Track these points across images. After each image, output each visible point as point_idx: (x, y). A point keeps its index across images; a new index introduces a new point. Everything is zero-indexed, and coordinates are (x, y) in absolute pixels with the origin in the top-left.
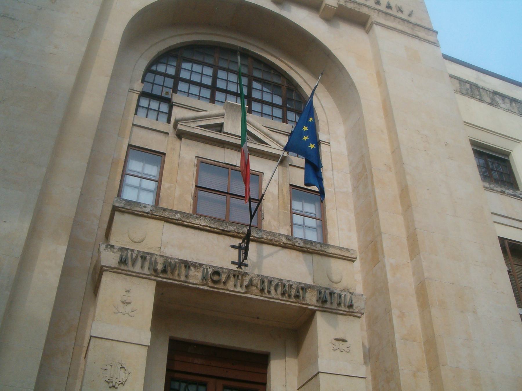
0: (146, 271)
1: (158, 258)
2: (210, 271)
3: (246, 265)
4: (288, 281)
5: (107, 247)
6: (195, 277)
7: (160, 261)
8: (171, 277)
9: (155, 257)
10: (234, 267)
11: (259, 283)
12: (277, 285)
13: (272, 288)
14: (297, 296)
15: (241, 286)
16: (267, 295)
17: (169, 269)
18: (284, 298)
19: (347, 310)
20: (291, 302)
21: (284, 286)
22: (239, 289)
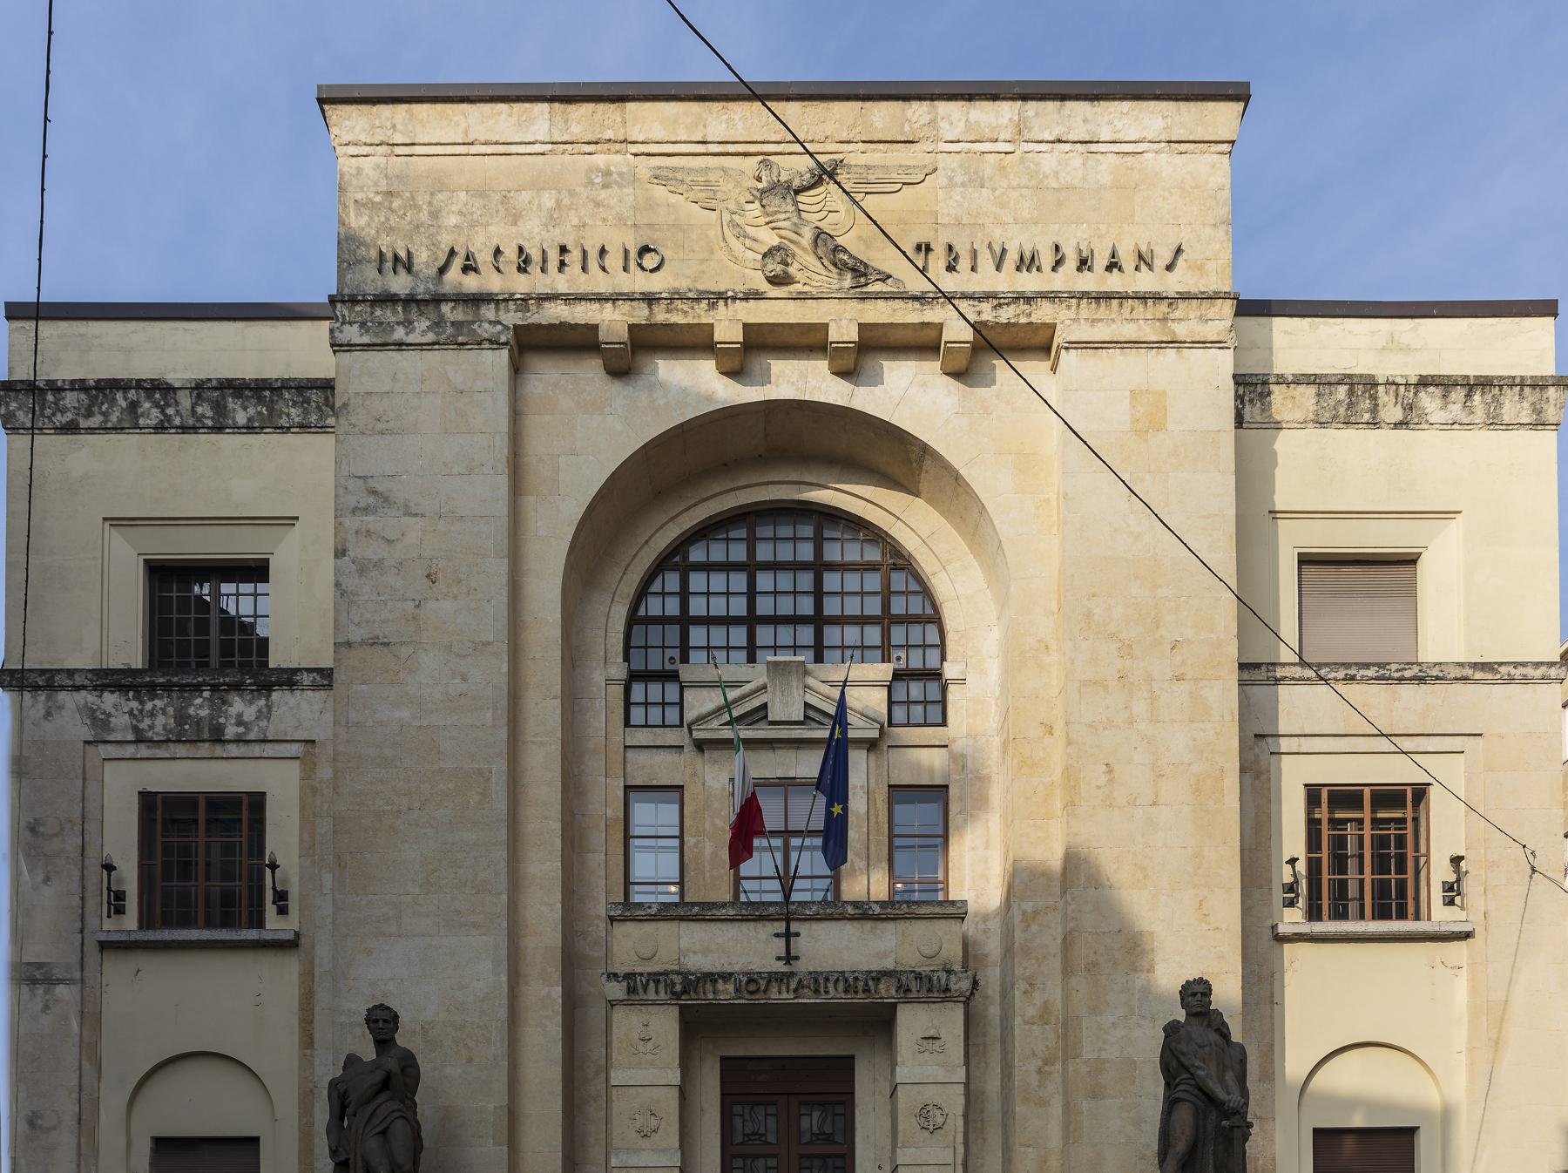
2: (744, 979)
3: (797, 958)
6: (726, 992)
7: (678, 979)
13: (831, 986)
14: (866, 990)
20: (861, 999)
22: (785, 995)
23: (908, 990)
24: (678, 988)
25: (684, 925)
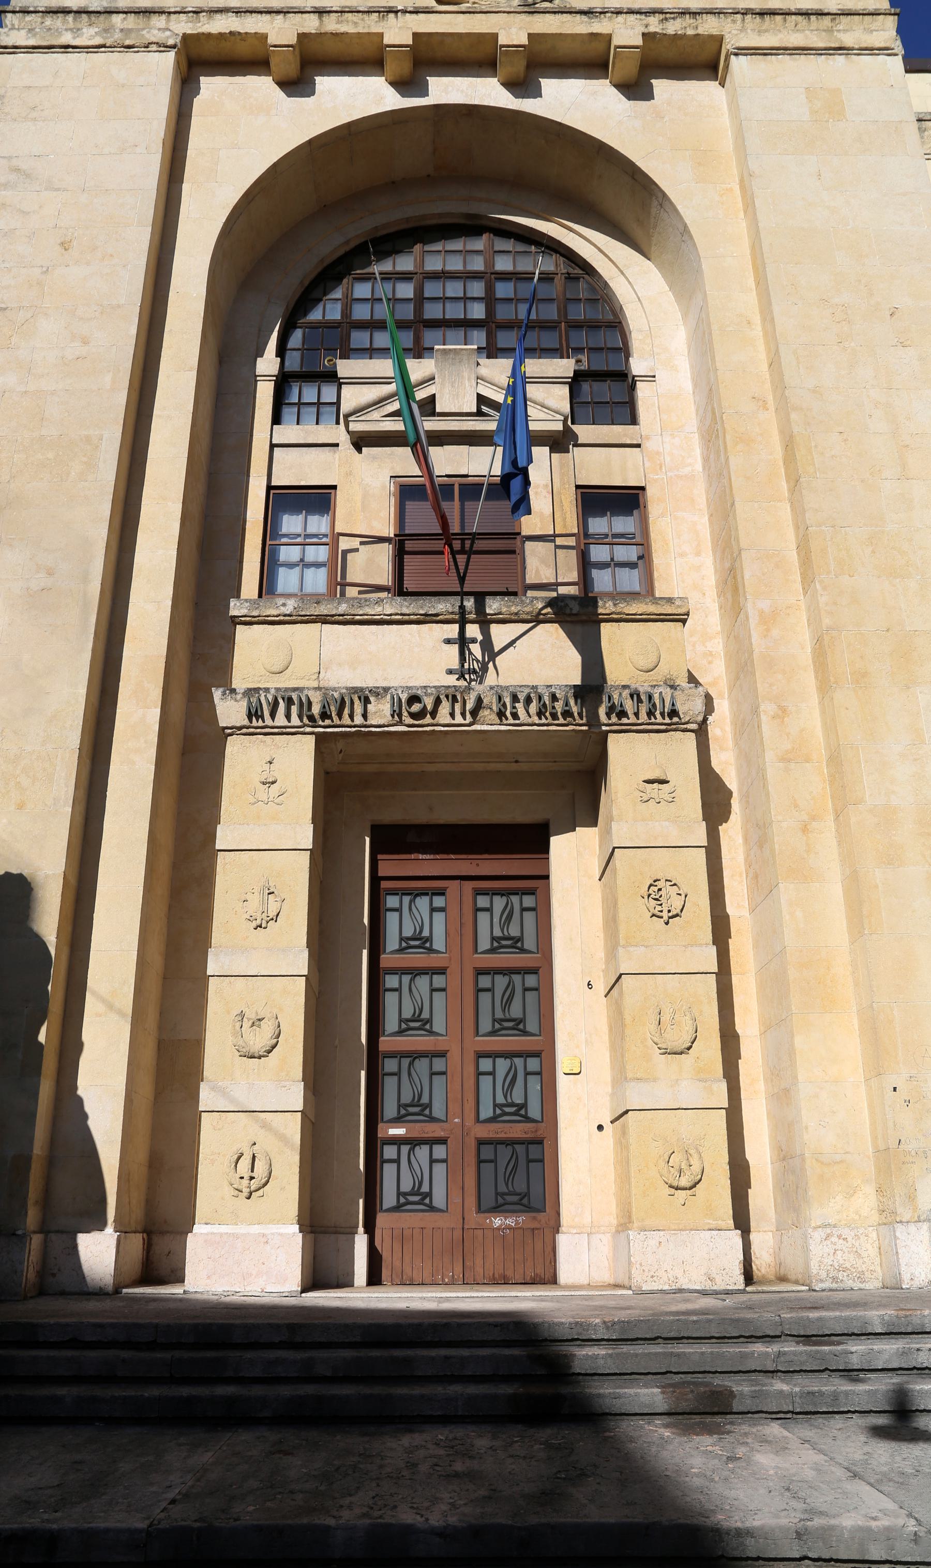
0: (295, 721)
1: (311, 694)
2: (404, 697)
4: (548, 686)
5: (224, 694)
6: (380, 713)
8: (339, 723)
9: (306, 692)
10: (452, 680)
11: (494, 700)
12: (528, 700)
13: (520, 707)
15: (463, 715)
16: (512, 721)
17: (333, 708)
18: (544, 721)
19: (667, 720)
21: (540, 698)
22: (459, 719)
23: (622, 714)
24: (316, 710)
25: (326, 627)
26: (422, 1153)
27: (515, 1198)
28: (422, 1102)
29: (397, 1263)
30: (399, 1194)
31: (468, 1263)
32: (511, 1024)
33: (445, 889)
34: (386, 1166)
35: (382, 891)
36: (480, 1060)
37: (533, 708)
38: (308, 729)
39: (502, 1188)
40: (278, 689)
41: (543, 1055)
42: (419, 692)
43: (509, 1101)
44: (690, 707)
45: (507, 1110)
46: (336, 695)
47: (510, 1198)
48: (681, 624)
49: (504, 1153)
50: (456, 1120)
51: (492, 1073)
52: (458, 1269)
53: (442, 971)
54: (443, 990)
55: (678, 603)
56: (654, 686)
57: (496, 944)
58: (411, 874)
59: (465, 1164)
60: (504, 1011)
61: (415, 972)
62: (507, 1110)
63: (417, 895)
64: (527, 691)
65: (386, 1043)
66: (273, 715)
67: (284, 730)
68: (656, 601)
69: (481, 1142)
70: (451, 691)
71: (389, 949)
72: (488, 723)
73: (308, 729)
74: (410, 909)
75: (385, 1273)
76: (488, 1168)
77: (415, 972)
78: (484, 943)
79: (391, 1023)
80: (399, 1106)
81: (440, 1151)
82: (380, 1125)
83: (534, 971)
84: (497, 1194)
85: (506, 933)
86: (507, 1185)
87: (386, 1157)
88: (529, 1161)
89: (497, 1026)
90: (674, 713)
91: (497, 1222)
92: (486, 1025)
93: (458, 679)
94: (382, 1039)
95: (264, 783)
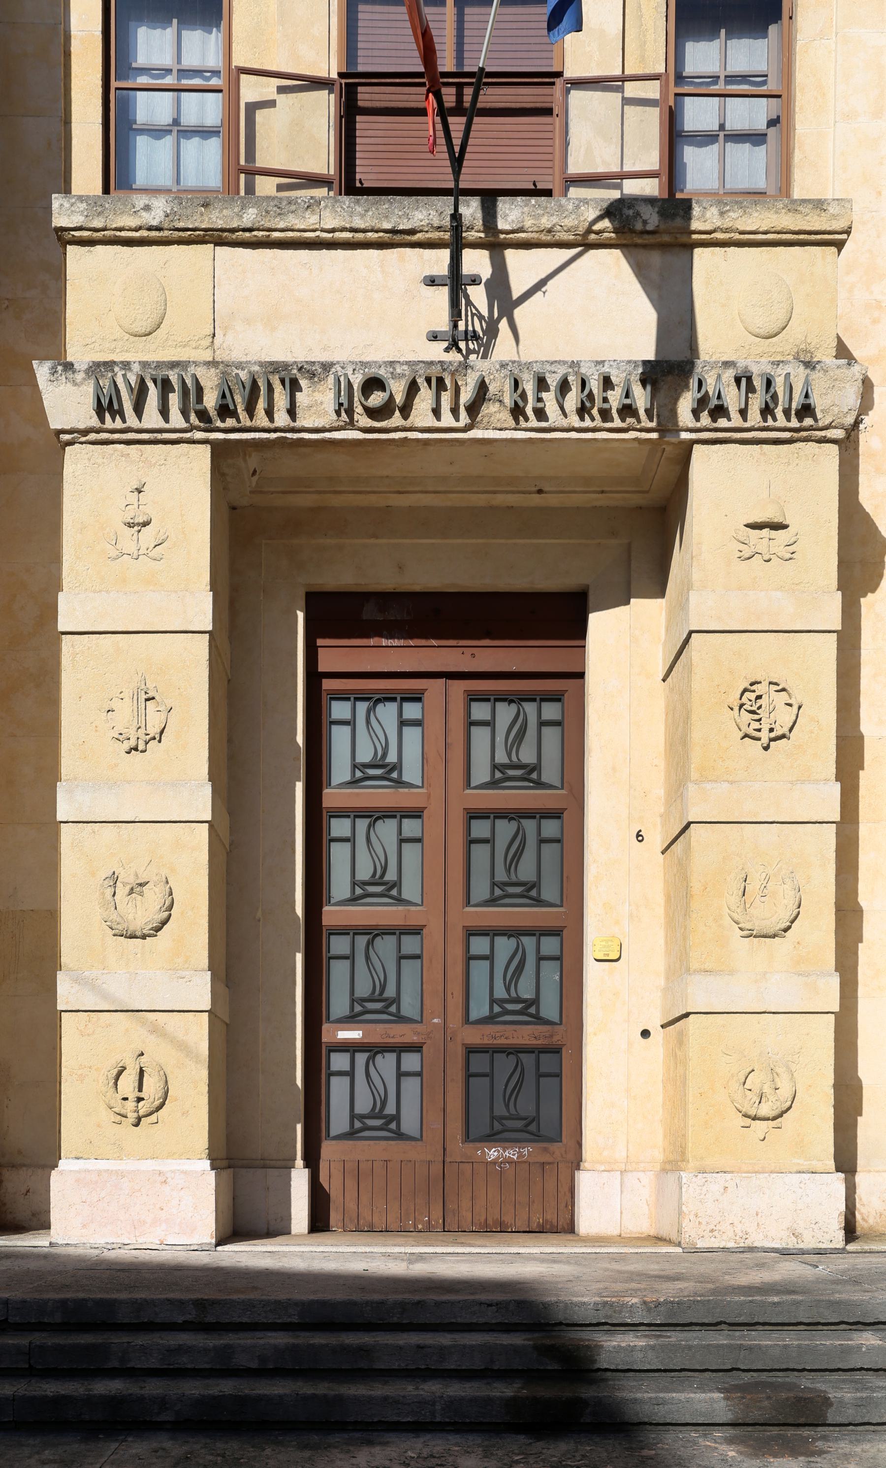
0: (177, 420)
2: (357, 381)
5: (54, 372)
6: (317, 407)
7: (210, 382)
8: (248, 423)
9: (192, 369)
10: (437, 352)
12: (564, 387)
13: (549, 398)
15: (455, 411)
17: (238, 399)
18: (588, 423)
19: (794, 423)
22: (447, 420)
23: (720, 411)
24: (210, 401)
26: (386, 1063)
27: (519, 1124)
28: (385, 995)
29: (351, 1205)
30: (353, 1116)
31: (450, 1206)
32: (518, 890)
33: (423, 692)
34: (334, 1080)
35: (324, 694)
36: (472, 938)
37: (572, 400)
38: (199, 435)
39: (500, 1110)
40: (144, 365)
41: (565, 932)
42: (382, 372)
43: (513, 994)
44: (834, 401)
45: (510, 1007)
46: (244, 375)
47: (510, 1124)
48: (834, 249)
49: (504, 1065)
50: (436, 1021)
51: (490, 958)
52: (437, 1214)
53: (416, 814)
54: (418, 840)
55: (833, 209)
56: (777, 363)
57: (498, 775)
58: (368, 669)
59: (448, 1079)
60: (508, 871)
61: (375, 815)
62: (510, 1007)
63: (378, 701)
64: (561, 371)
65: (331, 915)
66: (139, 410)
67: (159, 436)
68: (795, 205)
69: (471, 1051)
70: (435, 371)
71: (335, 781)
72: (495, 425)
73: (199, 435)
74: (368, 722)
75: (334, 1217)
76: (480, 1085)
77: (375, 815)
78: (481, 773)
79: (339, 885)
80: (353, 1001)
81: (411, 1061)
82: (325, 1027)
83: (556, 815)
84: (493, 1118)
85: (514, 758)
86: (507, 1106)
87: (334, 1067)
88: (540, 1075)
89: (498, 892)
90: (806, 410)
91: (493, 1154)
92: (481, 889)
93: (447, 350)
94: (326, 909)
95: (130, 525)
